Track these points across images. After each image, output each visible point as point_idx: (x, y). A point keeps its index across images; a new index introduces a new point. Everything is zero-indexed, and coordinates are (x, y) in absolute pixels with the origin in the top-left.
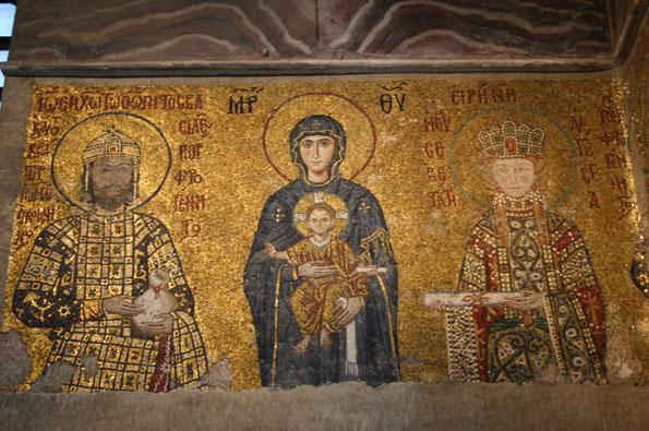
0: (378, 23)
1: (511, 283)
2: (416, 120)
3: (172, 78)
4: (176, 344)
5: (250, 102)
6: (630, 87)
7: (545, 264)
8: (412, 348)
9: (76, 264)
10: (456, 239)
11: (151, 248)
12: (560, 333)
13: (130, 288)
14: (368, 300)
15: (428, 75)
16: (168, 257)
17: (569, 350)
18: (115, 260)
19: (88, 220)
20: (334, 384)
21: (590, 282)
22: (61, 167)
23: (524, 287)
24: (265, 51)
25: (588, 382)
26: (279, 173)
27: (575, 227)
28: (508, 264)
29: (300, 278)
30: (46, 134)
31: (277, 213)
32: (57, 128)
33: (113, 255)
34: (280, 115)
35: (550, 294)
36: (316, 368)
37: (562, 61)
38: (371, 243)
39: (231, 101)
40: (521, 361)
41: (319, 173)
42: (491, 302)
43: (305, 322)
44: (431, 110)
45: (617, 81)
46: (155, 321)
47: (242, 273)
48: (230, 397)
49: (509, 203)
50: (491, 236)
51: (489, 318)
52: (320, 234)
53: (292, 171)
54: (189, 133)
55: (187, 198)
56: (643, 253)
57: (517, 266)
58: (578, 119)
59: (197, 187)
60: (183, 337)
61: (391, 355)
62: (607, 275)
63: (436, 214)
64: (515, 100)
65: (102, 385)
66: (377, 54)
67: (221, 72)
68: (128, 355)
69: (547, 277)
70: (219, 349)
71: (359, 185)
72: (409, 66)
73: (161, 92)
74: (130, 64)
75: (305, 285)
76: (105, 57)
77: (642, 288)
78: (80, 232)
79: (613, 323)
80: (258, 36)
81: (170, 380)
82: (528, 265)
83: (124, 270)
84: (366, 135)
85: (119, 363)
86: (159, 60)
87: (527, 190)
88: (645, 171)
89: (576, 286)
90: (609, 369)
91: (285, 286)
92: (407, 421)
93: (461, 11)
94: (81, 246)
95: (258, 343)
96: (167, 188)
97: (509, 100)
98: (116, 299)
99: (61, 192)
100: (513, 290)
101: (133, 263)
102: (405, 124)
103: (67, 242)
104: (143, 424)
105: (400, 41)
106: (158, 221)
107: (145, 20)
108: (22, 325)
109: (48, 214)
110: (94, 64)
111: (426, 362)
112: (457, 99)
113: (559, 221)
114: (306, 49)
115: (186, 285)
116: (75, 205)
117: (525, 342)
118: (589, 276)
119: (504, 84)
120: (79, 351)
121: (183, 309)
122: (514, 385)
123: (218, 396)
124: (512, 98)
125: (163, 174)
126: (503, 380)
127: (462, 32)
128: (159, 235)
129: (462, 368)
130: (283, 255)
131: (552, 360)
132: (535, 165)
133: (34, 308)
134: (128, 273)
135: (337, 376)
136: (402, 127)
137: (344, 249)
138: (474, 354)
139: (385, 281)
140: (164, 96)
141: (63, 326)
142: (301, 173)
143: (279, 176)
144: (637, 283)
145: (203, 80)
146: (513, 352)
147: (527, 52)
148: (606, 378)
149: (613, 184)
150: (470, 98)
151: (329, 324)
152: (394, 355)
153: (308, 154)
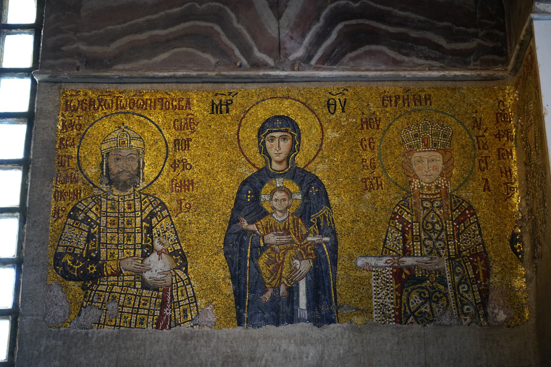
0: (327, 39)
1: (421, 249)
2: (354, 120)
3: (166, 85)
4: (174, 294)
5: (227, 105)
6: (519, 95)
7: (447, 235)
8: (347, 298)
9: (99, 232)
10: (384, 216)
11: (154, 220)
12: (455, 288)
13: (140, 251)
14: (315, 262)
15: (364, 83)
16: (167, 228)
17: (461, 301)
18: (128, 230)
19: (107, 199)
20: (290, 325)
21: (480, 249)
22: (85, 157)
23: (431, 253)
24: (238, 64)
25: (474, 324)
26: (250, 162)
27: (472, 206)
28: (420, 235)
29: (265, 245)
30: (72, 130)
31: (249, 194)
32: (80, 125)
33: (126, 226)
34: (251, 114)
35: (450, 259)
36: (277, 312)
37: (468, 73)
38: (318, 218)
39: (213, 103)
40: (425, 309)
41: (280, 162)
42: (406, 264)
43: (270, 278)
44: (366, 111)
45: (509, 89)
46: (159, 276)
47: (222, 241)
48: (214, 333)
49: (422, 187)
50: (408, 213)
51: (404, 276)
52: (280, 211)
53: (260, 161)
54: (181, 129)
55: (181, 182)
56: (520, 228)
57: (427, 237)
58: (478, 120)
59: (188, 173)
60: (180, 289)
61: (331, 304)
62: (492, 243)
63: (368, 196)
64: (431, 105)
65: (121, 325)
66: (325, 66)
67: (204, 80)
68: (140, 302)
69: (448, 245)
70: (206, 298)
71: (310, 172)
72: (349, 76)
73: (159, 96)
74: (135, 74)
75: (269, 250)
76: (115, 67)
77: (517, 254)
78: (101, 208)
79: (494, 280)
80: (233, 50)
81: (171, 320)
82: (434, 236)
83: (135, 238)
84: (316, 131)
85: (133, 308)
86: (157, 71)
87: (437, 176)
88: (526, 164)
89: (470, 253)
90: (490, 314)
91: (254, 250)
92: (342, 352)
93: (391, 29)
94: (103, 218)
95: (235, 293)
96: (165, 174)
97: (426, 105)
98: (130, 260)
99: (86, 177)
100: (422, 256)
101: (142, 232)
102: (346, 123)
103: (92, 215)
104: (152, 353)
105: (344, 55)
106: (159, 200)
107: (144, 36)
108: (61, 279)
109: (76, 194)
110: (108, 74)
111: (357, 309)
112: (386, 102)
113: (460, 201)
114: (270, 62)
115: (181, 250)
116: (97, 187)
117: (429, 294)
118: (479, 244)
119: (423, 91)
120: (104, 299)
121: (180, 268)
122: (421, 326)
123: (206, 333)
124: (428, 102)
125: (162, 163)
126: (412, 323)
127: (392, 47)
128: (161, 211)
129: (383, 313)
130: (253, 227)
131: (448, 309)
132: (443, 157)
133: (69, 266)
134: (138, 240)
135: (292, 319)
136: (343, 126)
137: (298, 223)
138: (392, 303)
139: (329, 249)
140: (162, 99)
141: (91, 280)
142: (266, 162)
143: (249, 165)
144: (514, 250)
145: (191, 86)
146: (421, 302)
147: (442, 64)
148: (487, 320)
149: (502, 172)
150: (396, 102)
151: (287, 280)
152: (334, 304)
153: (272, 148)
